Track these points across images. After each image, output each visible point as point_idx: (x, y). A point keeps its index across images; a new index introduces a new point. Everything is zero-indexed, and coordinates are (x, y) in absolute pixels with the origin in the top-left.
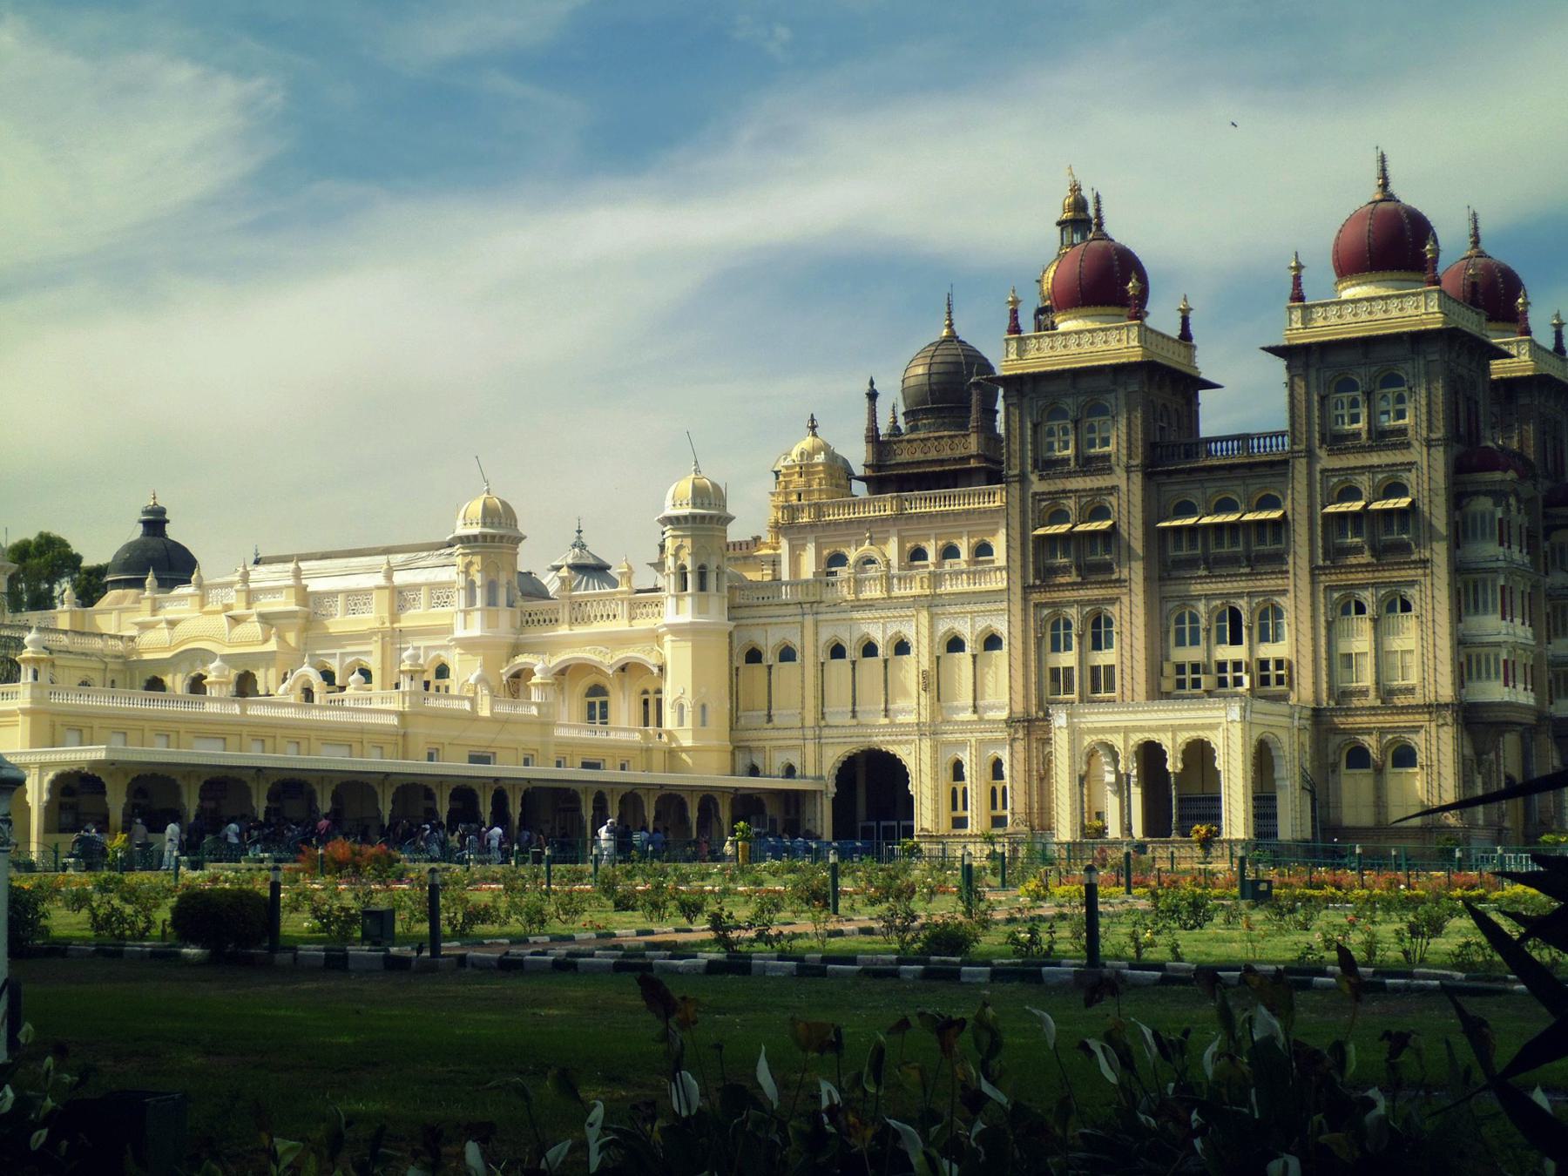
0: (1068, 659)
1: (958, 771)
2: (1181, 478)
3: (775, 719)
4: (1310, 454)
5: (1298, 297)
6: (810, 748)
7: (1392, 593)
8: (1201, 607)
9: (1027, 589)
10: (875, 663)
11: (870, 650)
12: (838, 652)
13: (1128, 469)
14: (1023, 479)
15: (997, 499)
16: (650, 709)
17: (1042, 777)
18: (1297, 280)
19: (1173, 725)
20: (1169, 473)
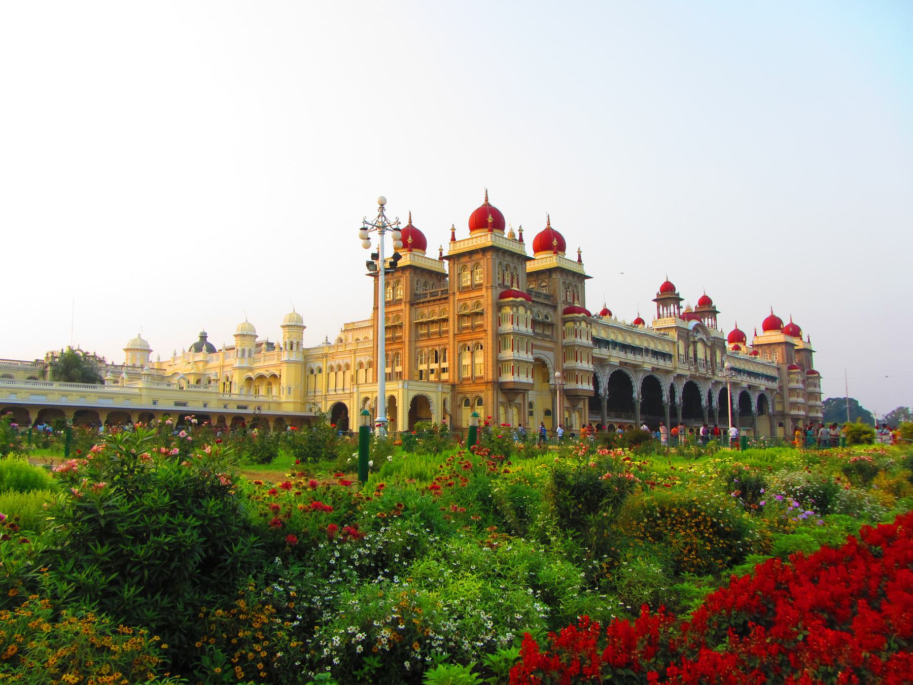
2: (421, 305)
4: (454, 293)
5: (453, 239)
7: (478, 343)
10: (341, 373)
11: (339, 367)
12: (332, 368)
18: (453, 234)
20: (418, 304)
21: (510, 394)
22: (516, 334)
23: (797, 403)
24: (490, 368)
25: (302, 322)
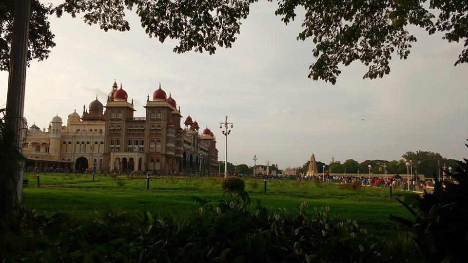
1: (95, 160)
5: (148, 100)
6: (73, 156)
8: (132, 140)
9: (108, 136)
11: (83, 143)
12: (78, 143)
13: (123, 121)
14: (108, 121)
15: (104, 123)
16: (47, 150)
17: (108, 162)
19: (128, 155)
21: (168, 157)
22: (173, 138)
23: (213, 161)
24: (164, 149)
25: (61, 120)
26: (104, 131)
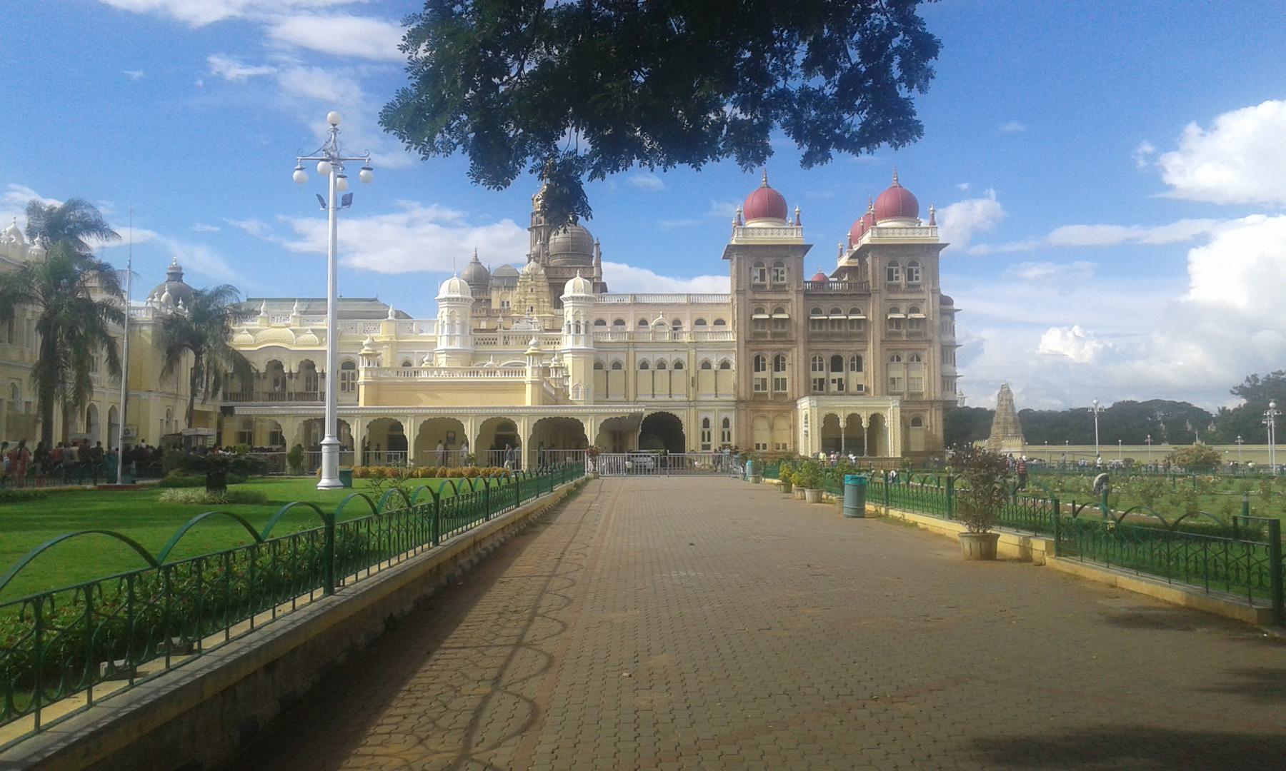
0: (761, 375)
1: (706, 423)
3: (610, 398)
8: (824, 354)
9: (747, 342)
10: (665, 373)
11: (661, 366)
12: (644, 366)
13: (797, 292)
26: (729, 326)
